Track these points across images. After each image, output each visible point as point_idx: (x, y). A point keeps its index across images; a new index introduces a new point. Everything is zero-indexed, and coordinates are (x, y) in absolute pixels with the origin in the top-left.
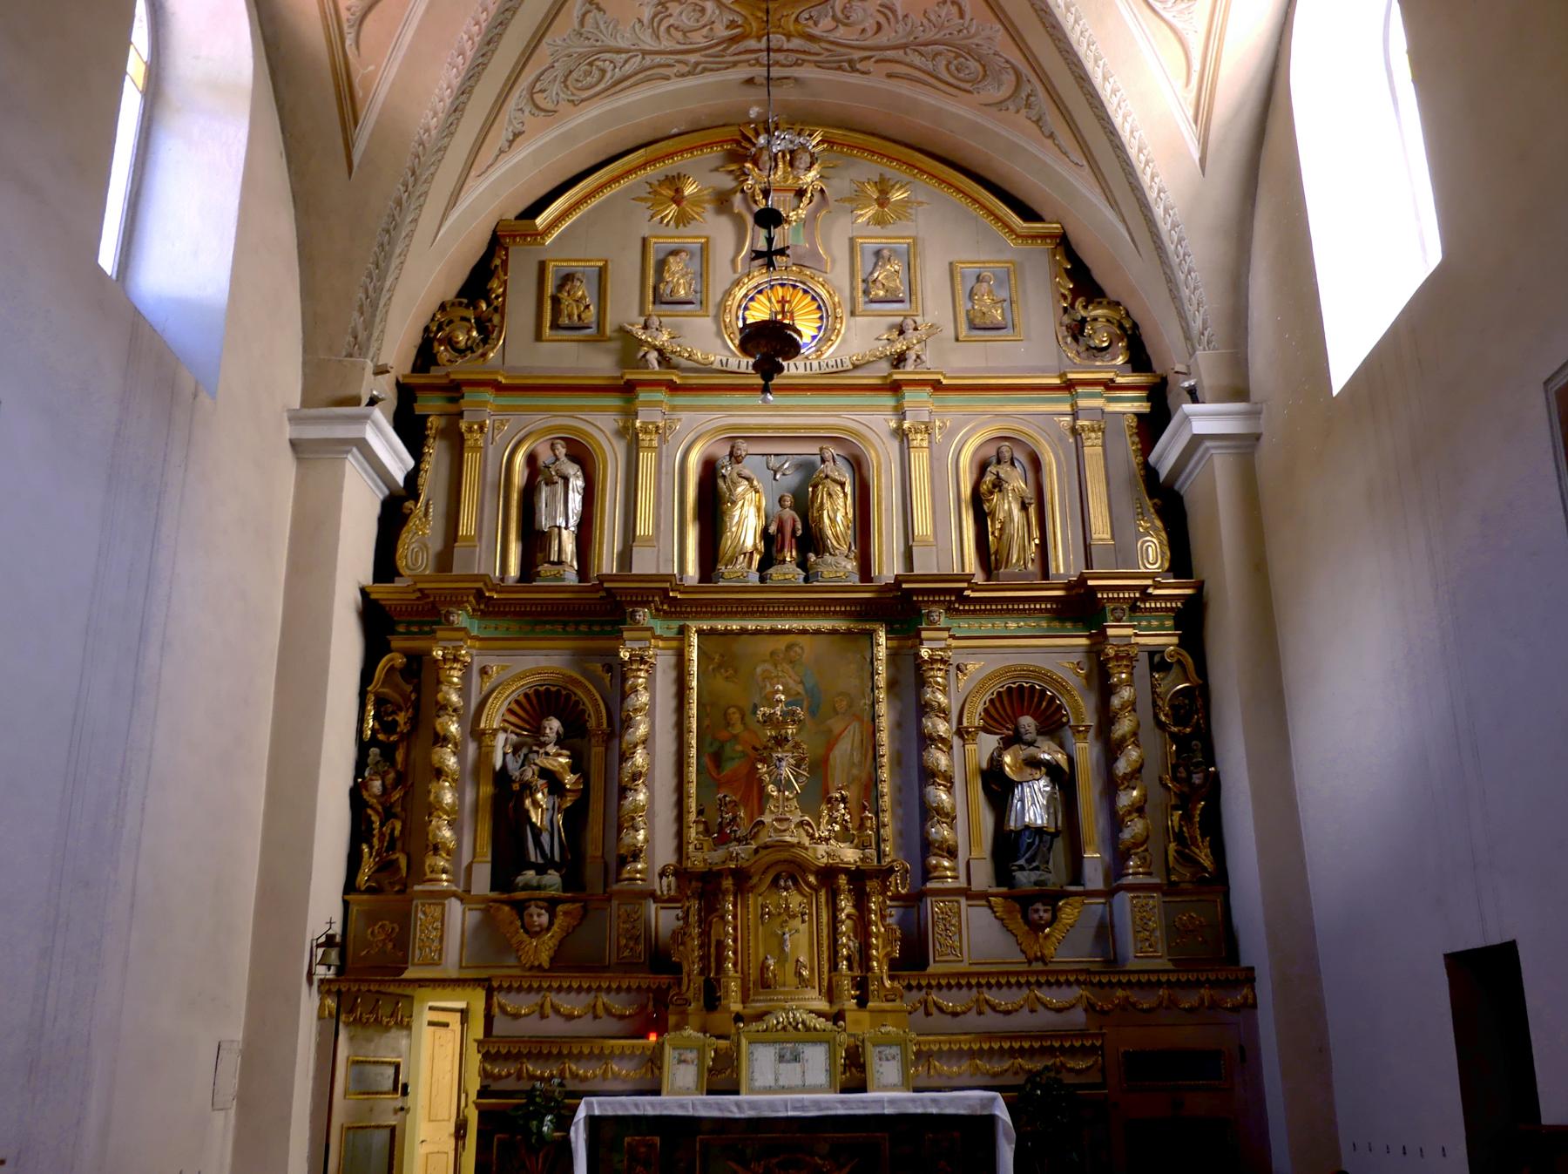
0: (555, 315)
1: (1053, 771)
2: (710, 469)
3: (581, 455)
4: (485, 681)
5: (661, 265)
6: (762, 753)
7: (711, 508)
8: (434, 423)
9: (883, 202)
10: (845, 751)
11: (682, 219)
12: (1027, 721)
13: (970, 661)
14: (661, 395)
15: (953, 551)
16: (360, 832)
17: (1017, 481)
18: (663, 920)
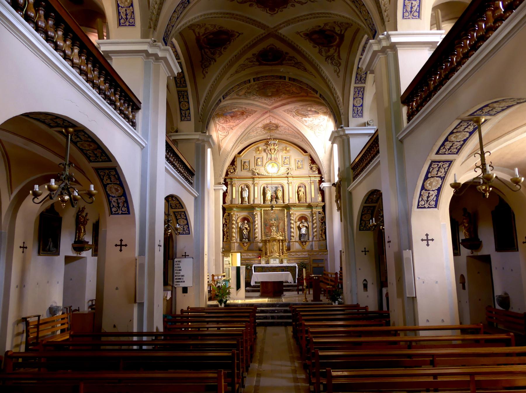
0: (243, 167)
1: (306, 227)
2: (264, 188)
3: (248, 187)
4: (238, 216)
5: (257, 160)
6: (271, 226)
7: (264, 194)
8: (229, 183)
9: (286, 150)
10: (281, 225)
11: (259, 154)
12: (303, 220)
13: (296, 213)
14: (258, 179)
15: (294, 200)
16: (224, 235)
17: (302, 190)
18: (260, 245)
